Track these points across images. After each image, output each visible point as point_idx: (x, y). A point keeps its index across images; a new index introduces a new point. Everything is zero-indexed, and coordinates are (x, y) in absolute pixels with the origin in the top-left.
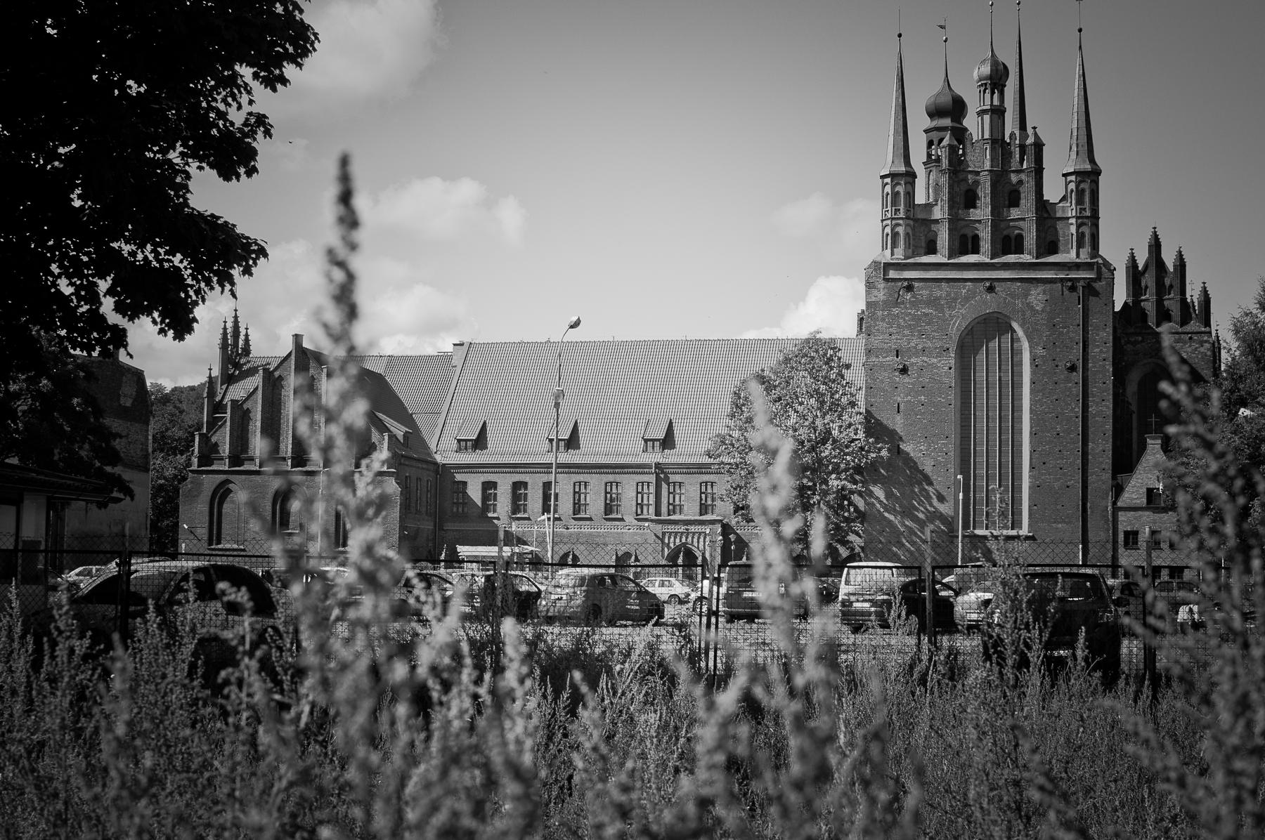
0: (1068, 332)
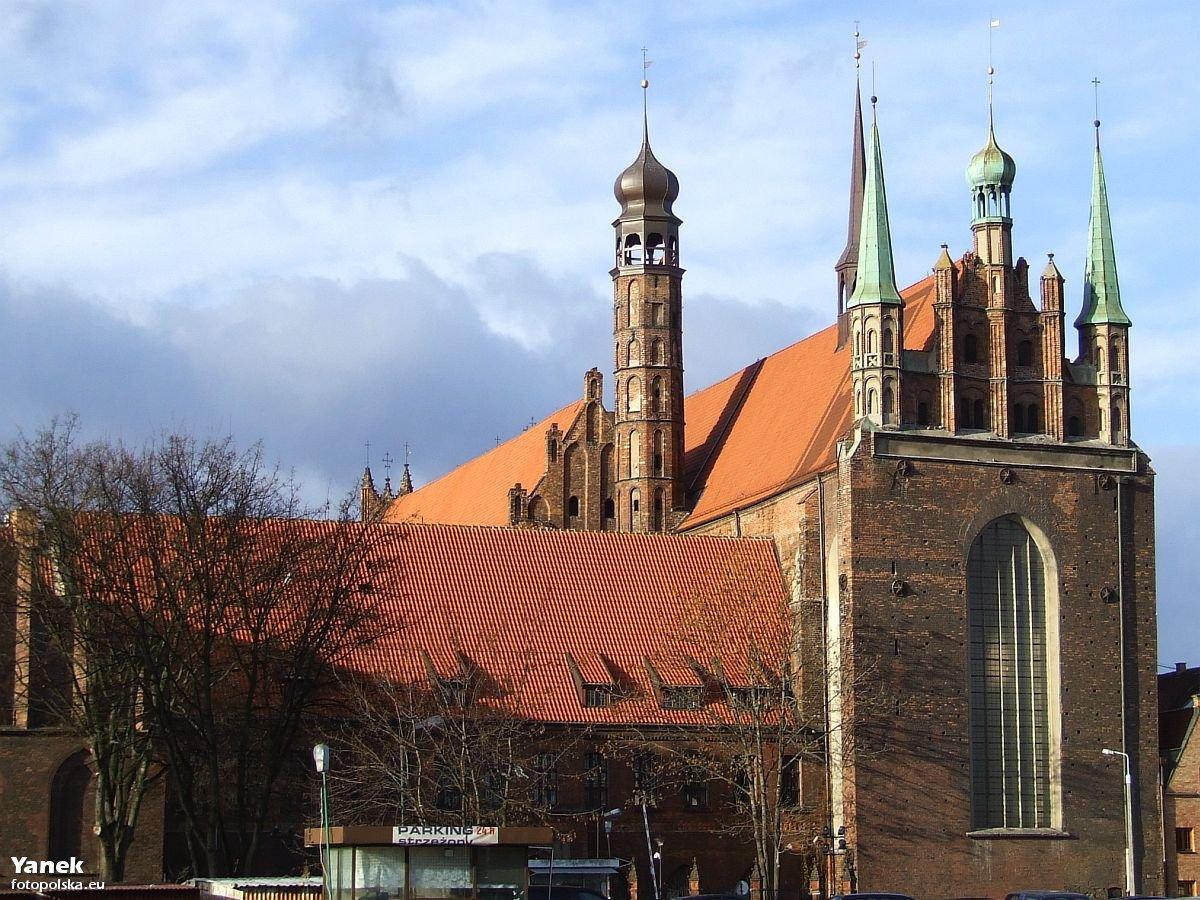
0: (1103, 547)
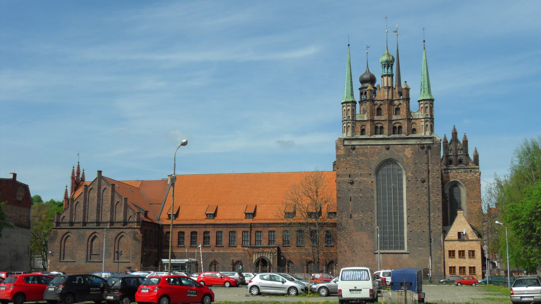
0: (422, 166)
